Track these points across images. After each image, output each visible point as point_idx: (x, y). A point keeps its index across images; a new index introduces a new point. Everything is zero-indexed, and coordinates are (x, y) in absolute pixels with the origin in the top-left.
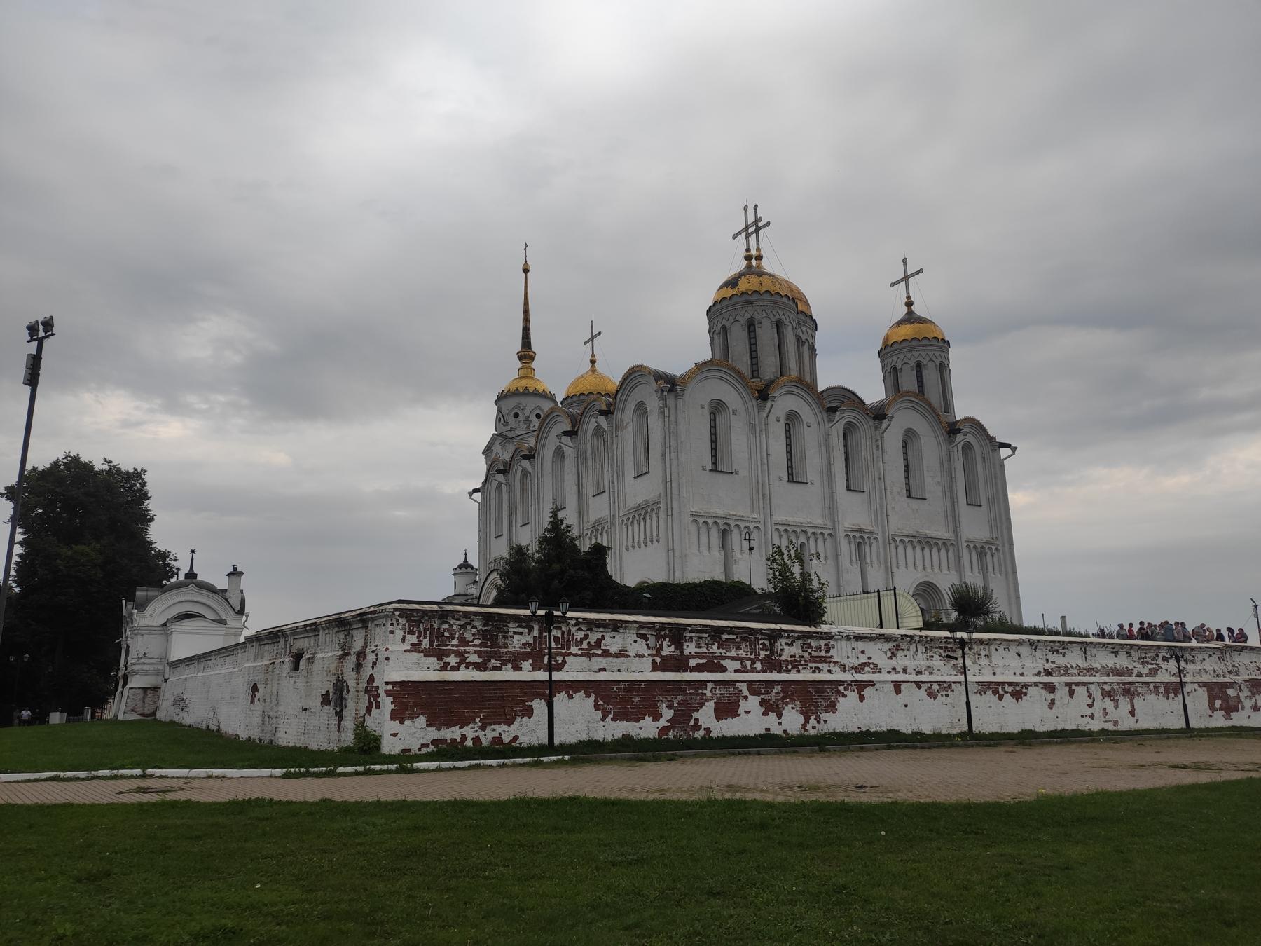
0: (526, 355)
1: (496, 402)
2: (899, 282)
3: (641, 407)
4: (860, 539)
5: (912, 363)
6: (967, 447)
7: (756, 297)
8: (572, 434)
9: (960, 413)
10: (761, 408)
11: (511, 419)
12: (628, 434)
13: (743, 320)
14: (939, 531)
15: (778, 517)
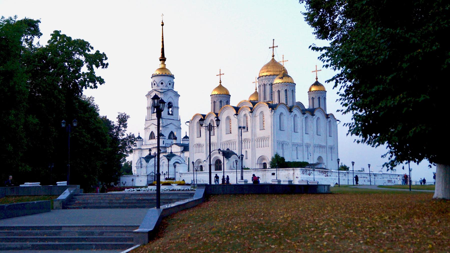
0: (163, 59)
1: (152, 78)
2: (315, 71)
3: (262, 112)
4: (308, 146)
5: (318, 97)
6: (330, 121)
7: (288, 84)
8: (237, 114)
9: (328, 112)
10: (290, 114)
11: (160, 85)
12: (258, 119)
13: (285, 89)
14: (323, 144)
15: (293, 141)
